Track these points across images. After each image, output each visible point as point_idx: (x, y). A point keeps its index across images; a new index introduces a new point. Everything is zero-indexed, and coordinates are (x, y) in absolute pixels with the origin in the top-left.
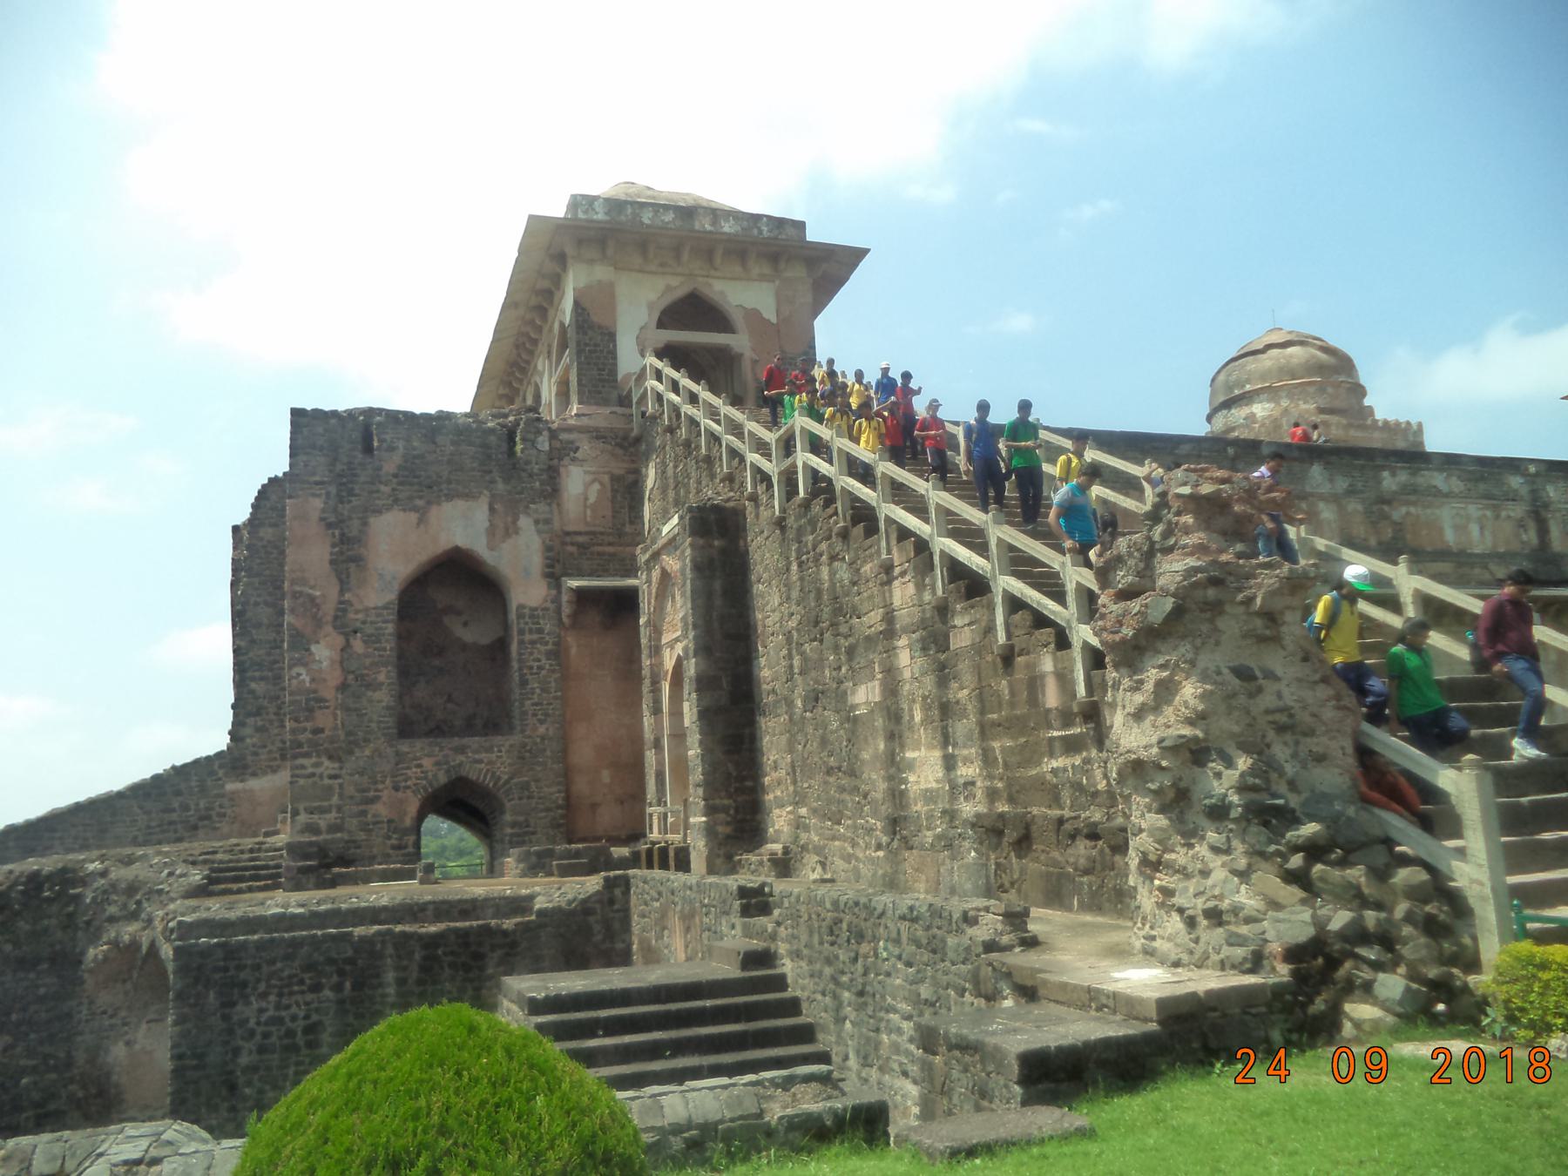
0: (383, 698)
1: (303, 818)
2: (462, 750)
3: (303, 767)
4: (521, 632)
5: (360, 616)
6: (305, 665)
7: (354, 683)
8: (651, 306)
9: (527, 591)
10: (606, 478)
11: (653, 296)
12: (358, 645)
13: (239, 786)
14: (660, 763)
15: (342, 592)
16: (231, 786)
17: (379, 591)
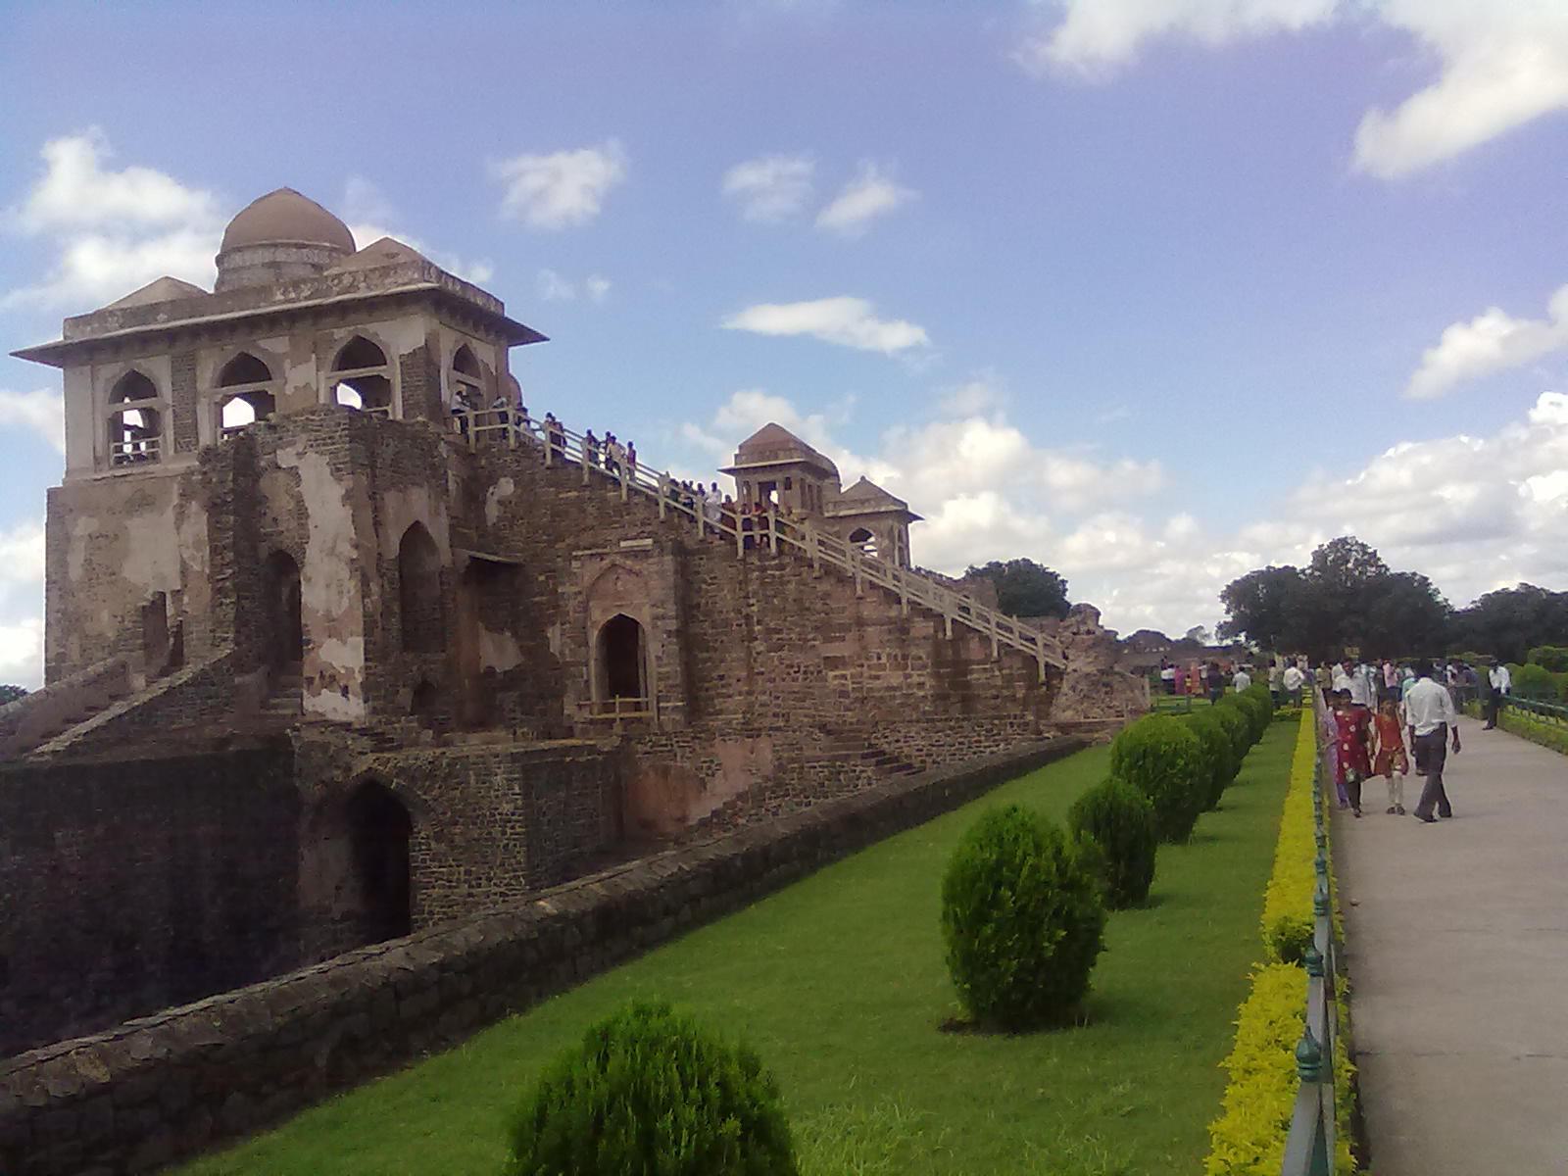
0: (395, 622)
1: (370, 703)
2: (425, 661)
3: (370, 668)
4: (442, 584)
5: (385, 565)
6: (369, 597)
7: (386, 613)
8: (451, 351)
9: (444, 554)
10: (459, 480)
11: (451, 346)
12: (386, 586)
13: (241, 679)
14: (588, 674)
15: (379, 546)
16: (237, 680)
17: (393, 548)
